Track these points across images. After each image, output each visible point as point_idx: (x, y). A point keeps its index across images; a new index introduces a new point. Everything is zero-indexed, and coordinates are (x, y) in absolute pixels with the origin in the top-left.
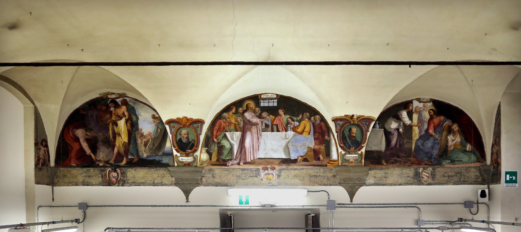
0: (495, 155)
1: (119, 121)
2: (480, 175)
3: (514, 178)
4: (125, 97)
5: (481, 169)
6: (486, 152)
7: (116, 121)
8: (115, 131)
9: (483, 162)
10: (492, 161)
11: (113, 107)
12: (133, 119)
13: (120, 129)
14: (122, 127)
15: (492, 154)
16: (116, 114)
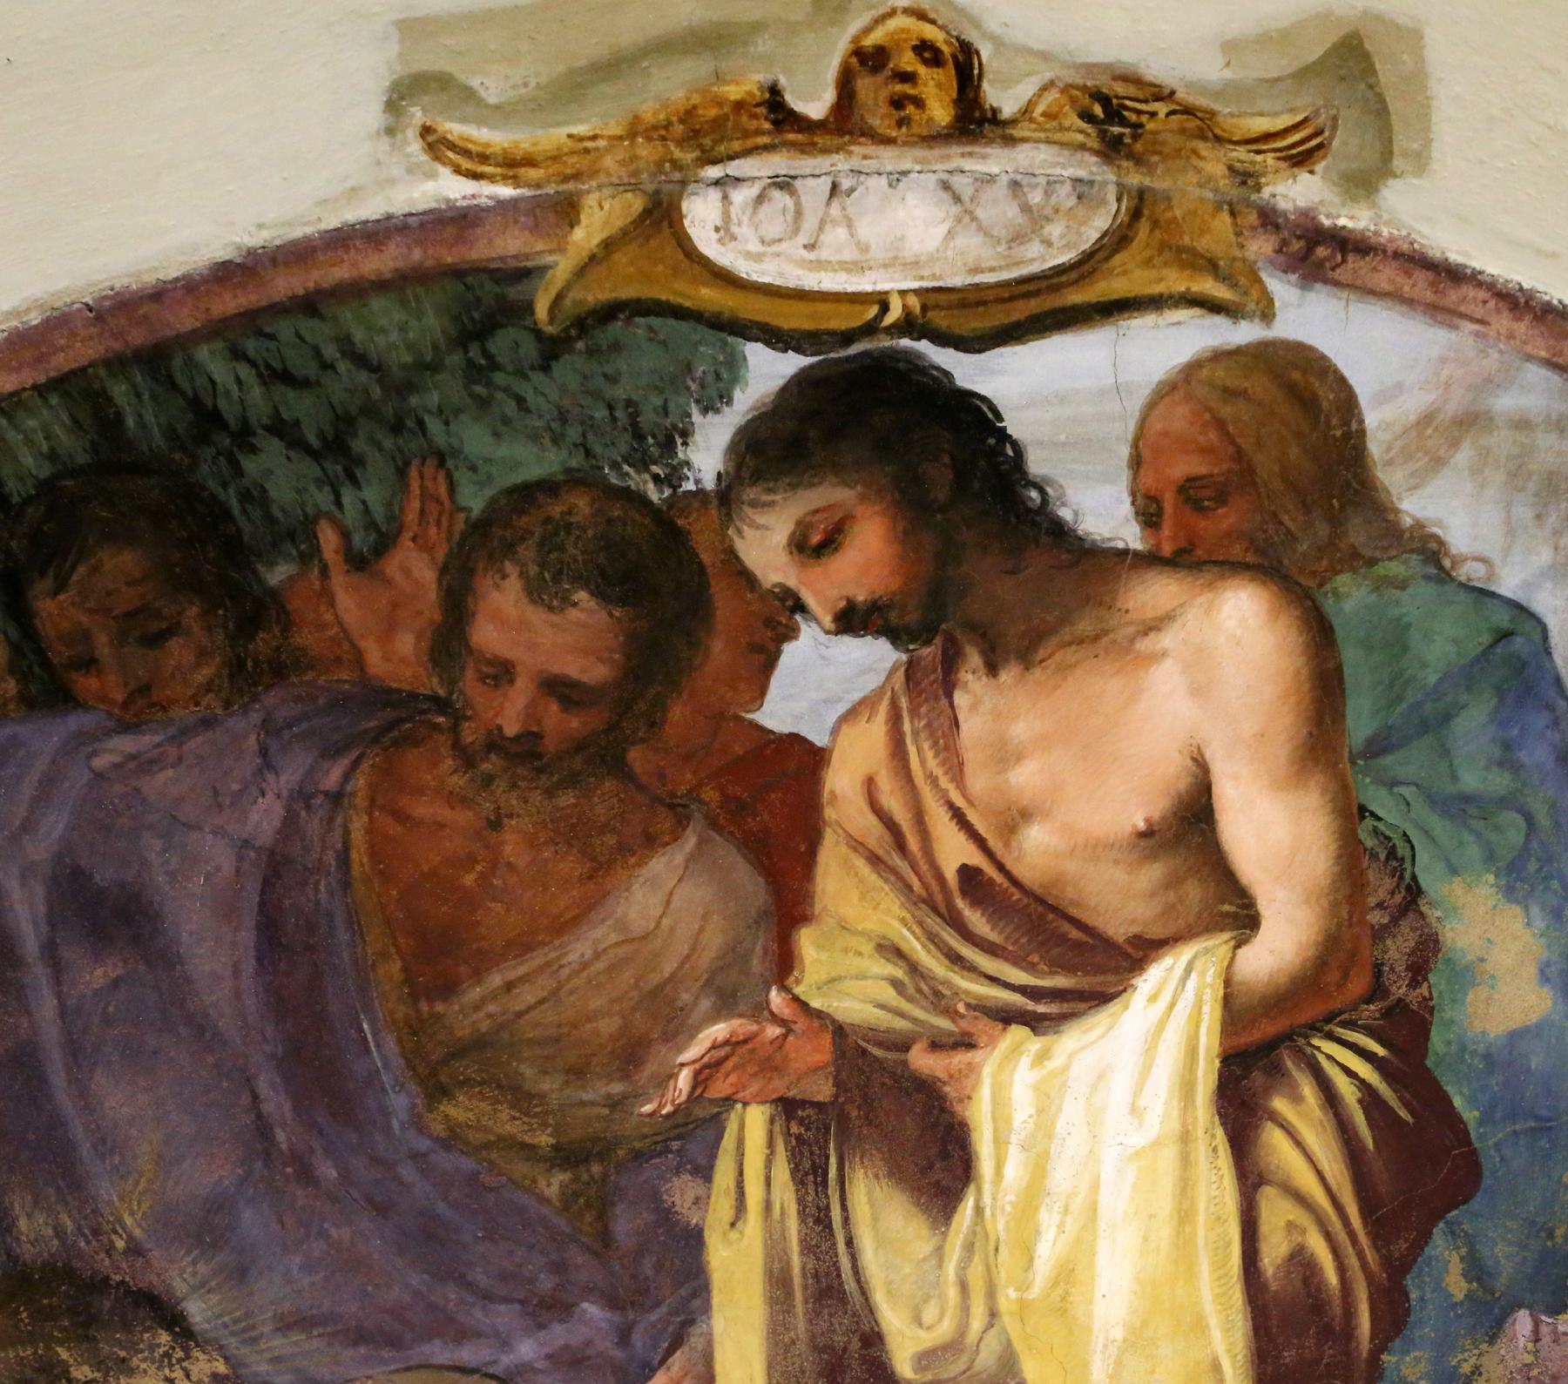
1: (1018, 1032)
4: (1281, 288)
7: (921, 1060)
8: (873, 1339)
11: (851, 620)
12: (1466, 976)
13: (1047, 1251)
14: (1115, 1201)
16: (954, 851)
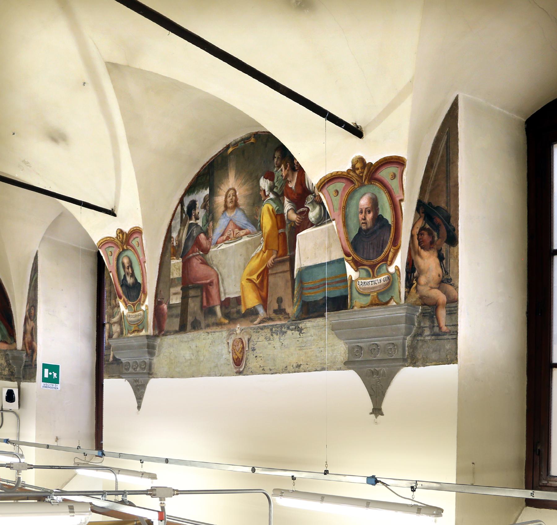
0: (28, 336)
2: (5, 364)
3: (55, 375)
5: (7, 354)
6: (16, 328)
9: (11, 343)
10: (24, 344)
15: (25, 333)
